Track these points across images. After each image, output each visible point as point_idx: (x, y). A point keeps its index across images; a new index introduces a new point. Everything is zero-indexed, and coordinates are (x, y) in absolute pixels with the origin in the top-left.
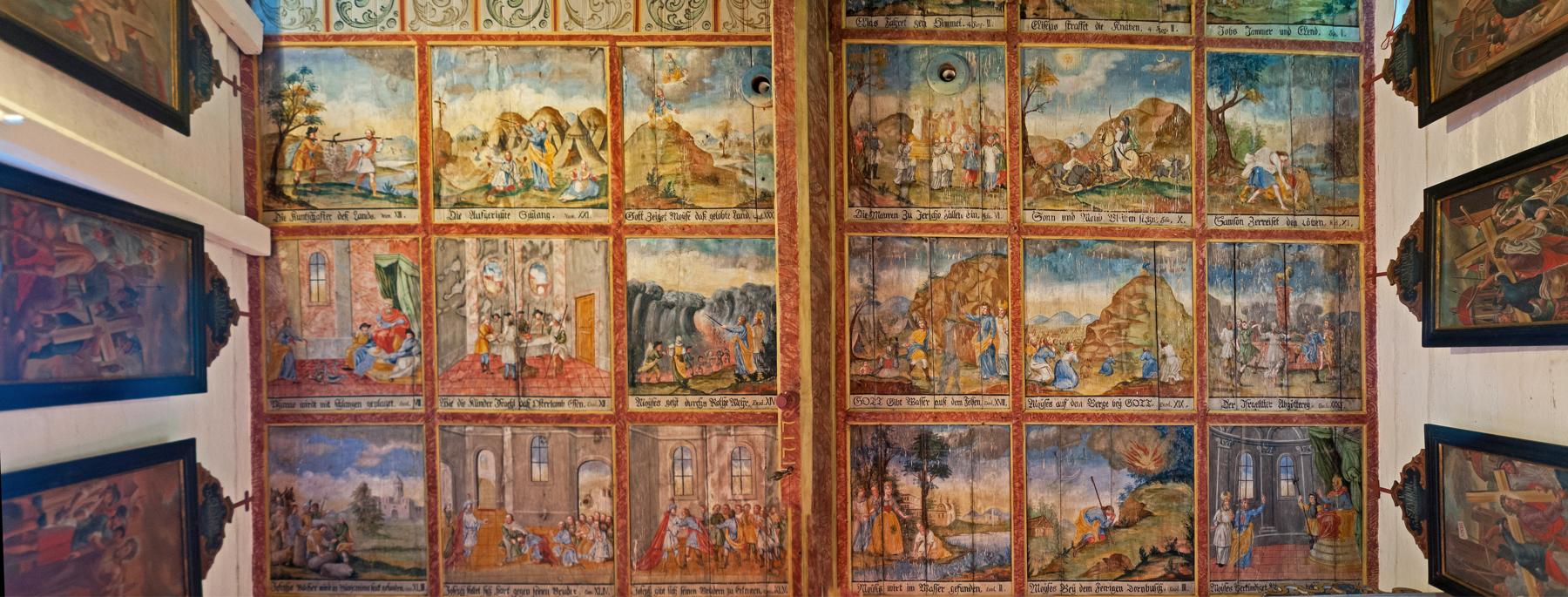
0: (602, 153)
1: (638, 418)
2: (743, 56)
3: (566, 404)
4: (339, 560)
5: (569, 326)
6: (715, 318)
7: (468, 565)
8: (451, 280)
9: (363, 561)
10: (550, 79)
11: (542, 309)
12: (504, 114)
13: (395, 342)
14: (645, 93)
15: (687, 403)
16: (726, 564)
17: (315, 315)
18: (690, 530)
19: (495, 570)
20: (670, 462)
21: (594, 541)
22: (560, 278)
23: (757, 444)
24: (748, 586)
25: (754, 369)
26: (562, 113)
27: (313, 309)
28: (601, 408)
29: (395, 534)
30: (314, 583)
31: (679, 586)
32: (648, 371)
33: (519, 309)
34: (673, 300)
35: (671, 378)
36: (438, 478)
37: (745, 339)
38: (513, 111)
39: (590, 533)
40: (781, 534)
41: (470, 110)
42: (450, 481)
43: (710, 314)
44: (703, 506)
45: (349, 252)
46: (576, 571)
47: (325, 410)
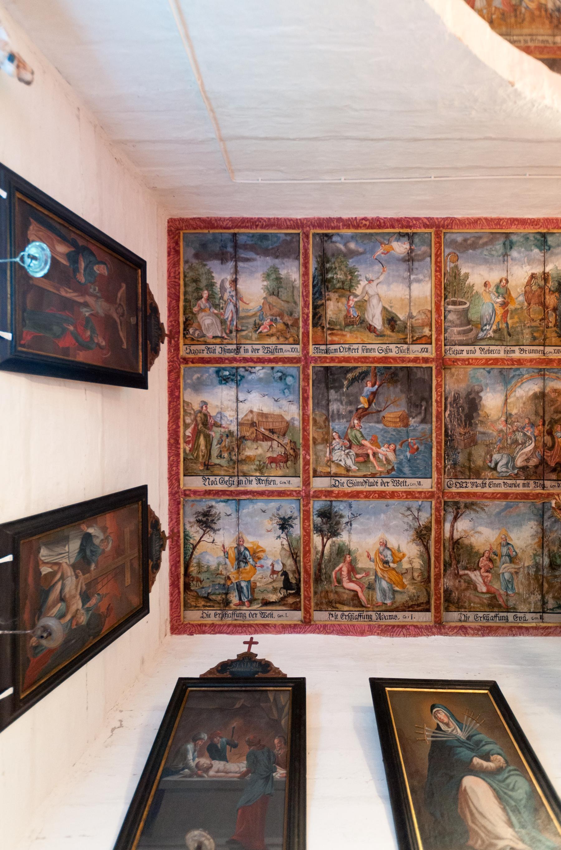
16: (523, 20)
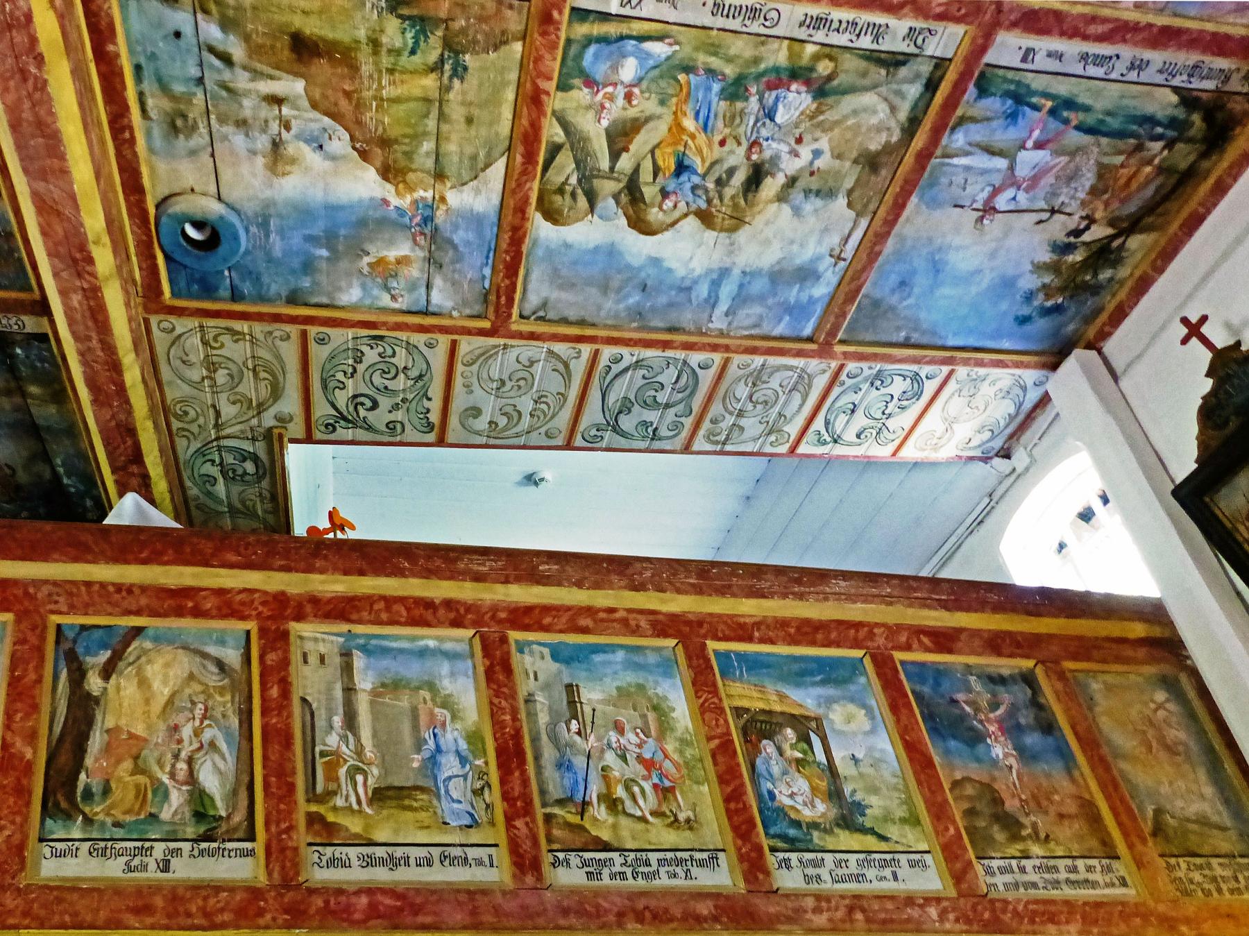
0: (558, 134)
2: (247, 288)
10: (629, 279)
12: (733, 230)
14: (450, 242)
26: (623, 221)
38: (715, 234)
41: (792, 242)
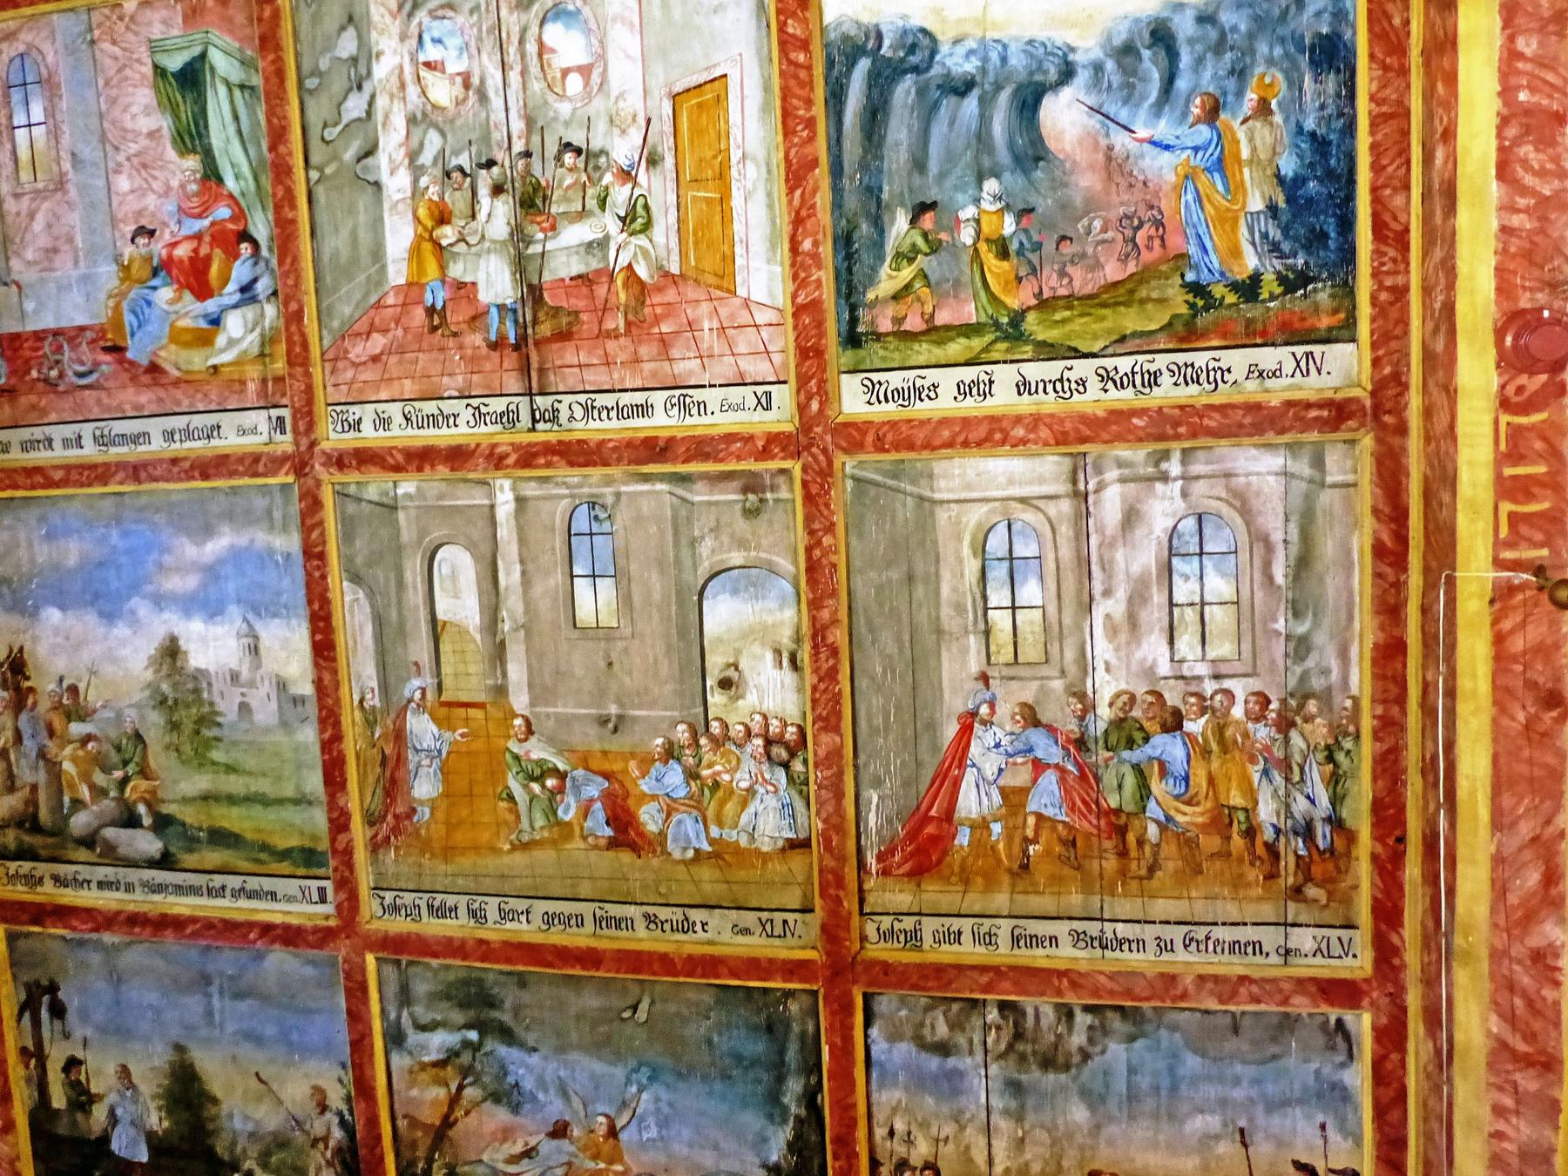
1: (870, 438)
3: (659, 409)
4: (132, 821)
5: (657, 182)
6: (1111, 109)
7: (425, 846)
8: (338, 85)
9: (183, 824)
11: (578, 138)
13: (215, 269)
15: (1023, 387)
16: (1152, 869)
17: (32, 216)
18: (1039, 767)
19: (489, 863)
20: (972, 566)
21: (751, 791)
22: (624, 43)
23: (1256, 504)
24: (1220, 933)
25: (1251, 261)
27: (25, 202)
28: (760, 415)
29: (250, 762)
30: (84, 872)
31: (1005, 926)
32: (896, 297)
33: (518, 146)
34: (971, 66)
35: (970, 312)
36: (337, 621)
37: (1220, 165)
39: (745, 770)
40: (1335, 780)
42: (369, 630)
43: (1092, 100)
44: (1081, 696)
45: (93, 42)
46: (706, 873)
47: (73, 454)
